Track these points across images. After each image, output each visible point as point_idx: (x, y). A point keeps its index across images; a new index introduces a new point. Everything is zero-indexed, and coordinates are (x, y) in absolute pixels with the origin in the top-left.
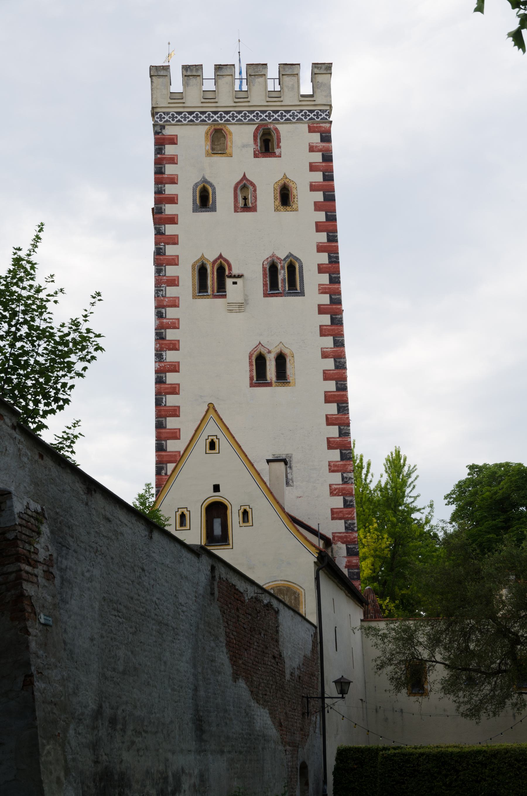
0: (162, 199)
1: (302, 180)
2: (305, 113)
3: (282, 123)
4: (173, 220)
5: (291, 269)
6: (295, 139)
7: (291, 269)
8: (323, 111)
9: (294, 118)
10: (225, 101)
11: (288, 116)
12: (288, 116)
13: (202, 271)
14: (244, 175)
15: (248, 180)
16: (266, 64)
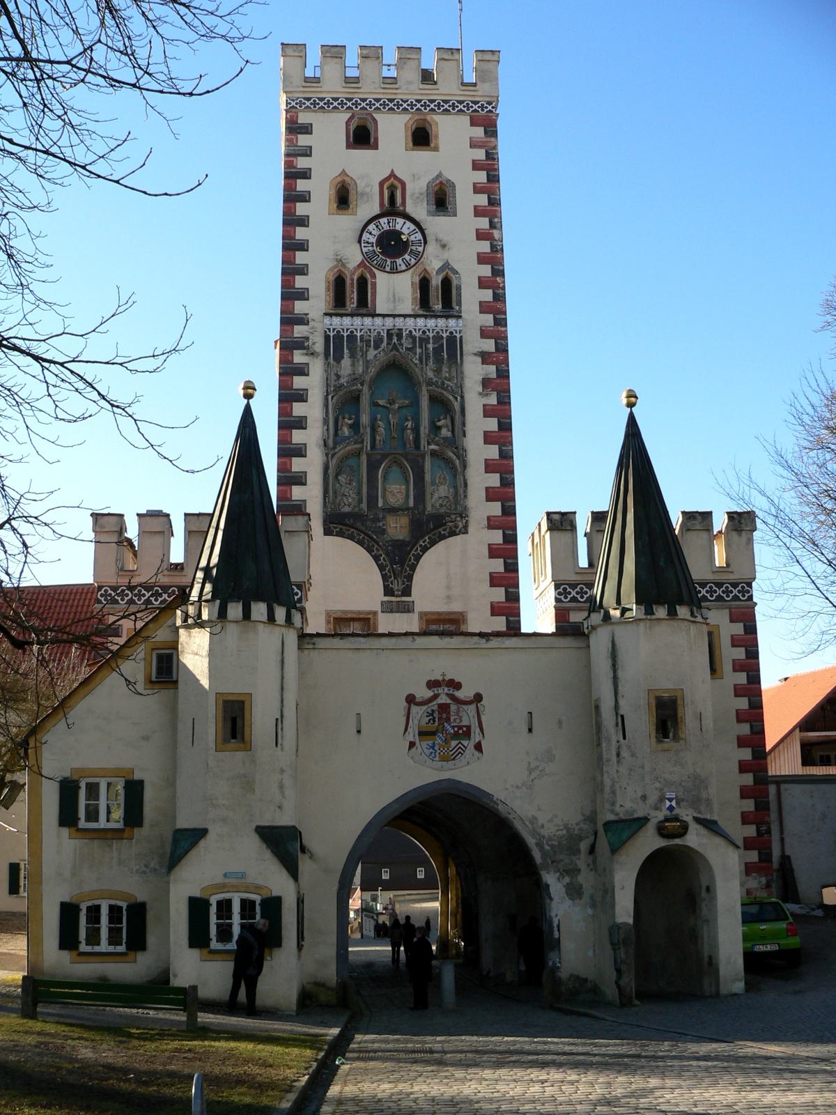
0: (292, 197)
1: (465, 181)
2: (468, 104)
3: (439, 114)
4: (304, 222)
5: (446, 283)
6: (454, 132)
7: (446, 283)
8: (489, 103)
9: (454, 109)
10: (370, 89)
11: (447, 107)
12: (447, 107)
13: (339, 286)
14: (392, 171)
15: (396, 178)
16: (420, 48)
